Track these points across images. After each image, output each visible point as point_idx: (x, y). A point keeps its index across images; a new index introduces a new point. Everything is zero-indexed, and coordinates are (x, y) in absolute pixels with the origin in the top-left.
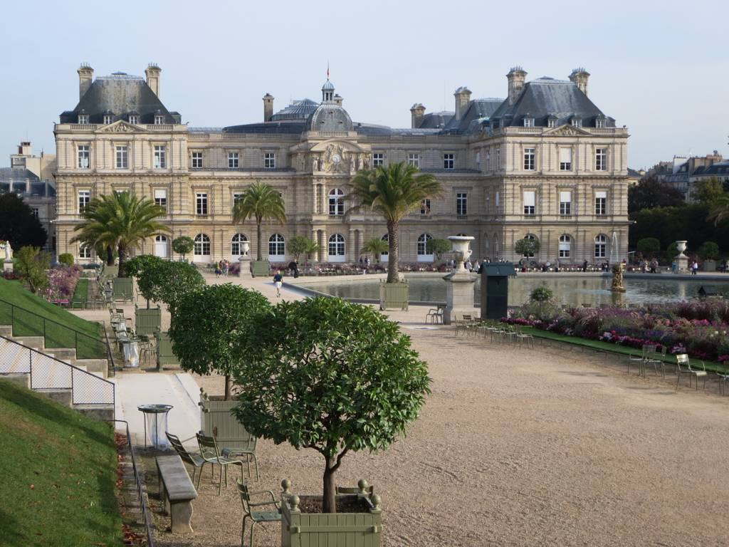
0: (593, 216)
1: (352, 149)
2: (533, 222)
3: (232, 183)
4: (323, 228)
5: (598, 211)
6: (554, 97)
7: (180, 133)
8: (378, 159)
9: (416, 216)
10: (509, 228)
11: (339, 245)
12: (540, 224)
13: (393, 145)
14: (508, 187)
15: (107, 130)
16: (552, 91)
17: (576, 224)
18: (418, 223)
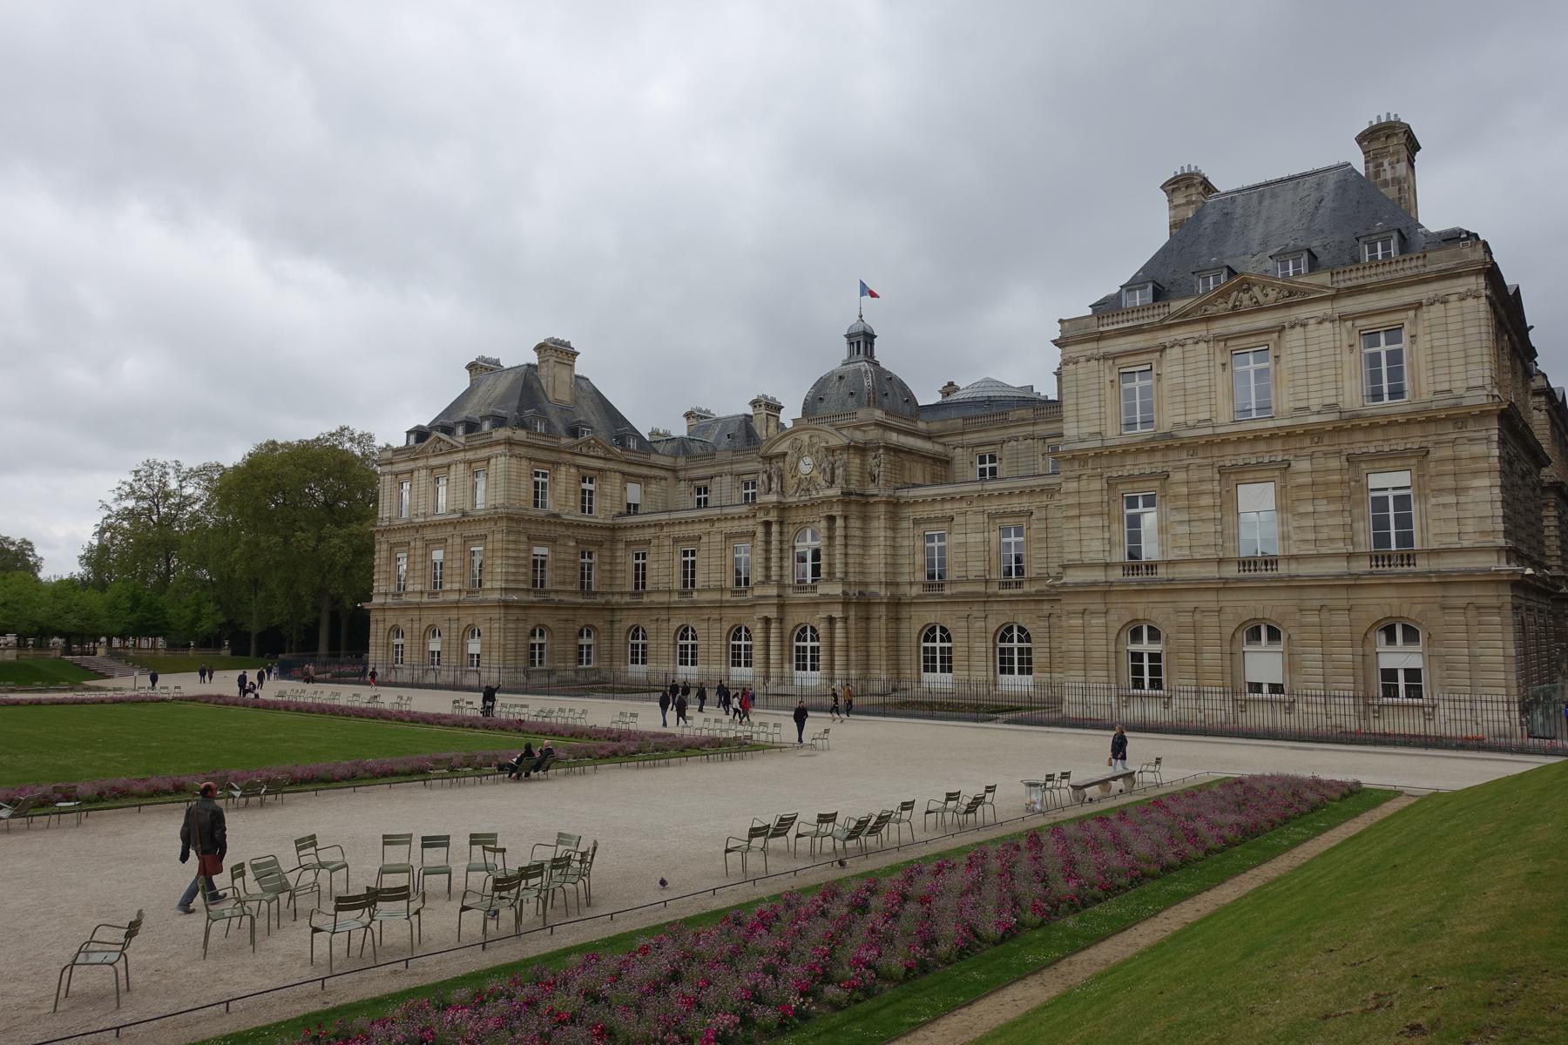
0: (1350, 556)
1: (835, 441)
2: (1140, 583)
3: (678, 531)
4: (772, 613)
5: (1381, 540)
6: (1264, 214)
7: (498, 443)
8: (988, 465)
9: (987, 581)
10: (1078, 604)
11: (813, 648)
12: (1172, 588)
13: (1013, 432)
14: (1073, 486)
15: (422, 451)
16: (1266, 203)
17: (1294, 584)
18: (986, 600)
